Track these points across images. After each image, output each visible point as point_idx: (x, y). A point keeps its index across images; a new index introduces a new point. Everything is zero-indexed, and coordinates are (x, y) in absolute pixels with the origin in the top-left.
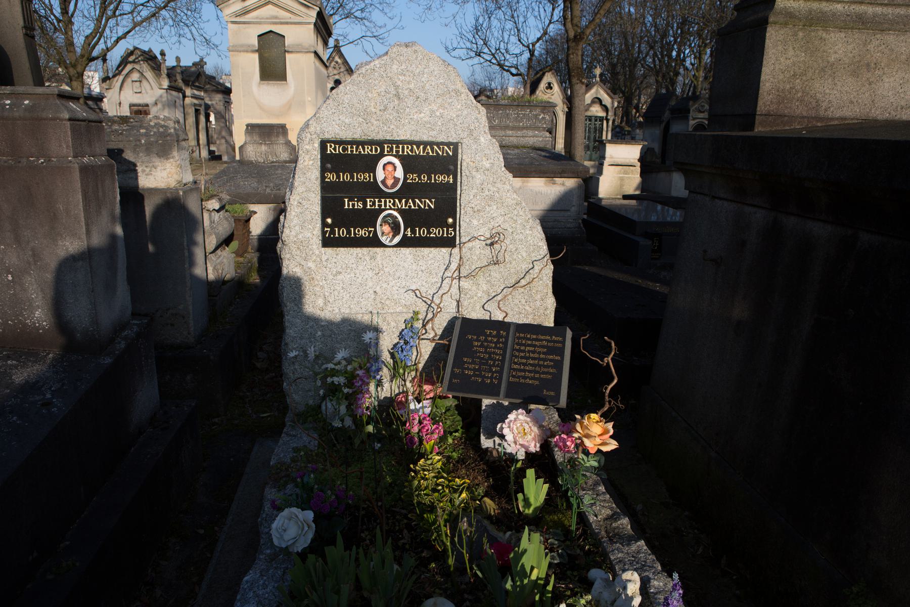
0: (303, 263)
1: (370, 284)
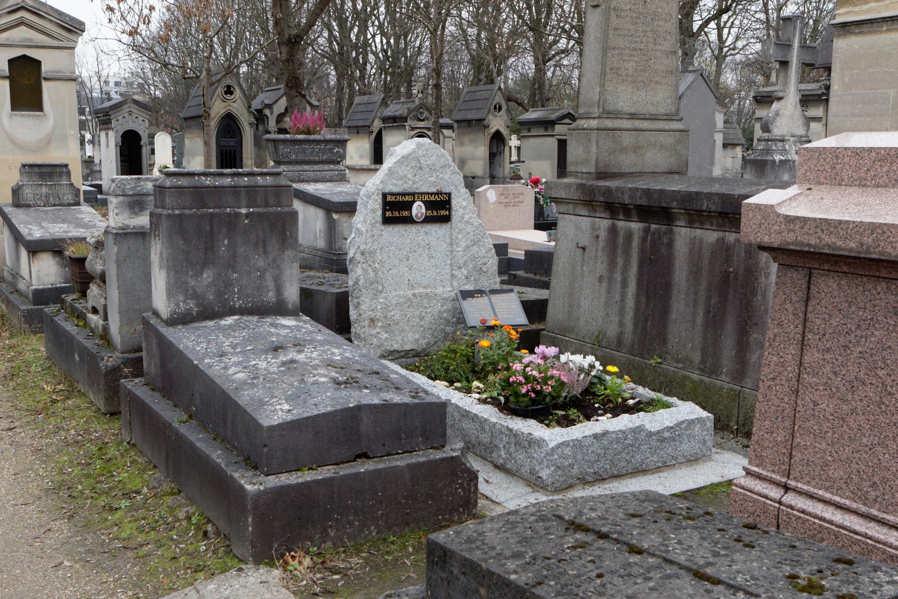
0: (372, 264)
1: (406, 275)
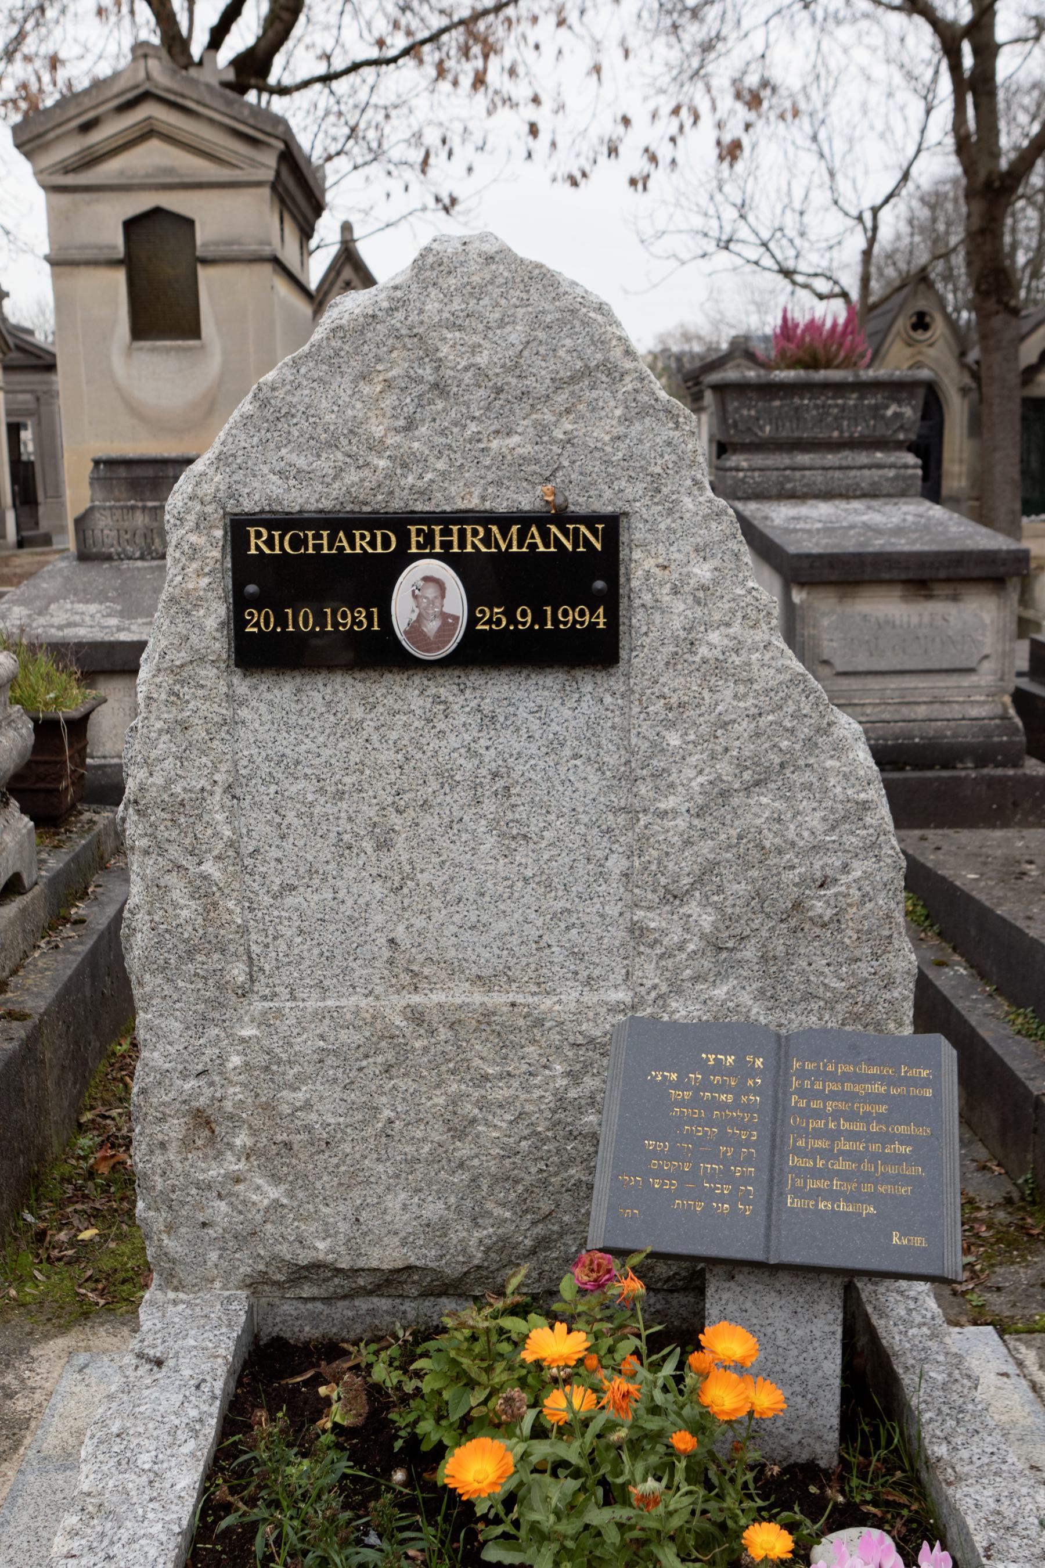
1: (379, 919)
